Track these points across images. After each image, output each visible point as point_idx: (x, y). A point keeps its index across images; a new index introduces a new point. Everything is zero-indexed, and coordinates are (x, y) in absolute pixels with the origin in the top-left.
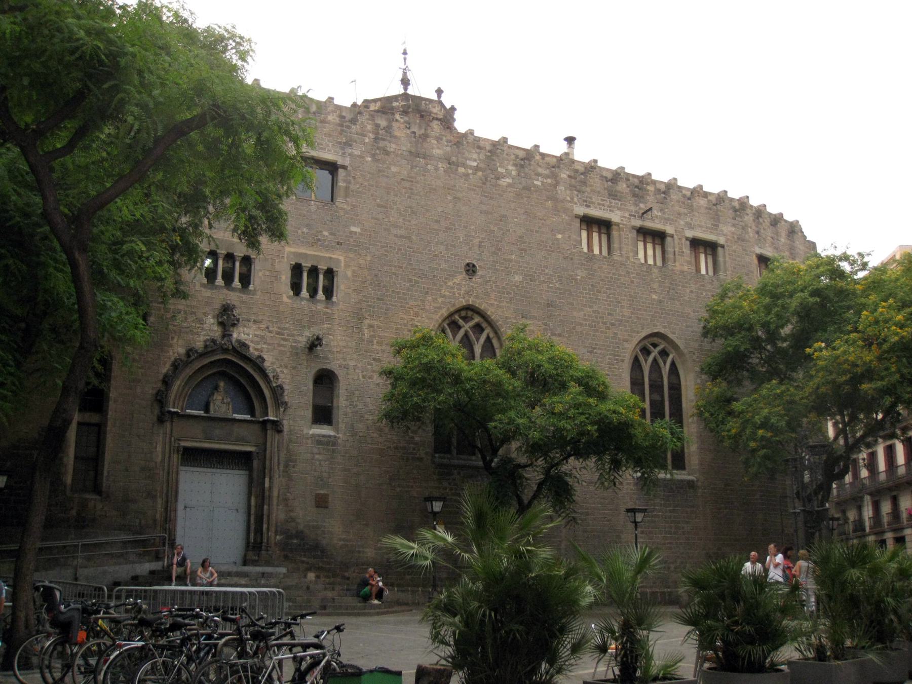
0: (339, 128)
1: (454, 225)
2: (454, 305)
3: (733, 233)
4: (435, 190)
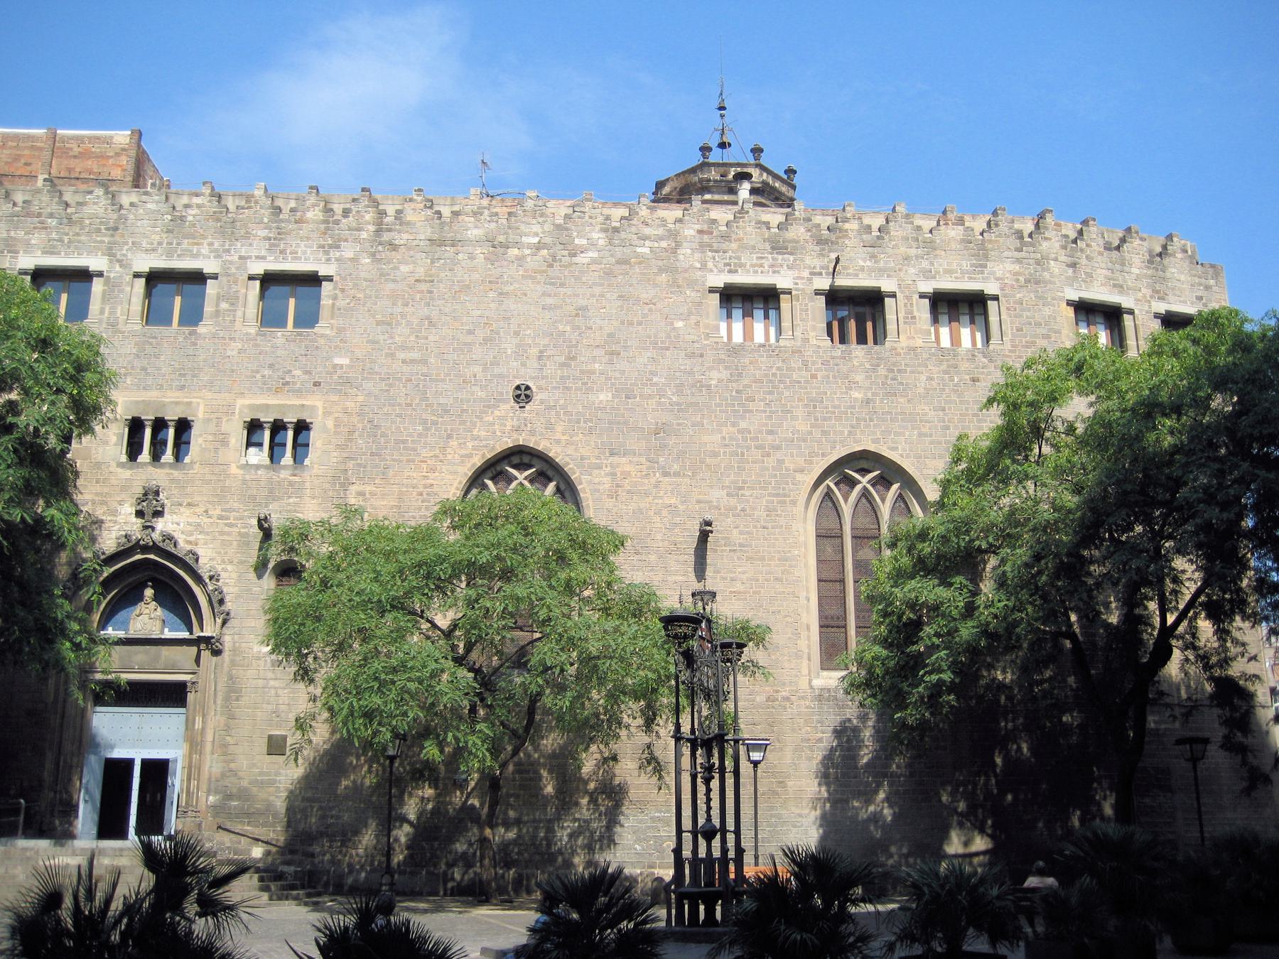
0: (323, 226)
1: (498, 333)
2: (493, 448)
3: (1016, 274)
4: (468, 287)
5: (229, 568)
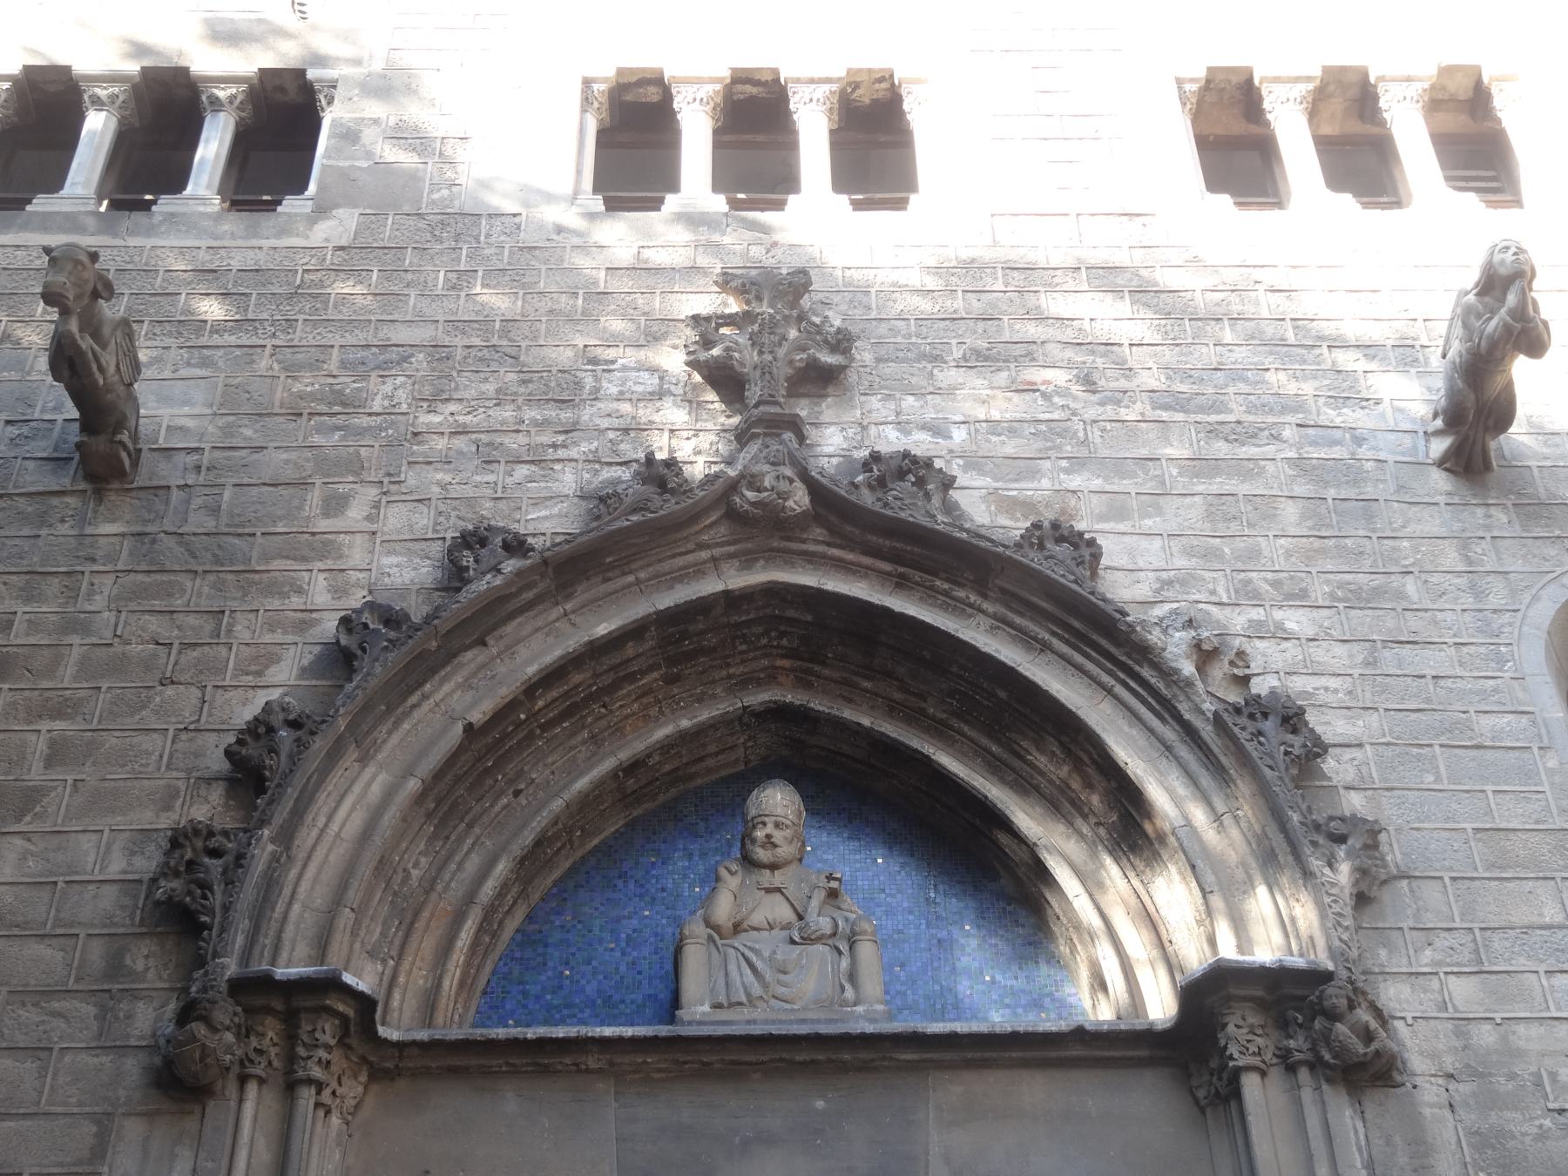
5: (1295, 620)
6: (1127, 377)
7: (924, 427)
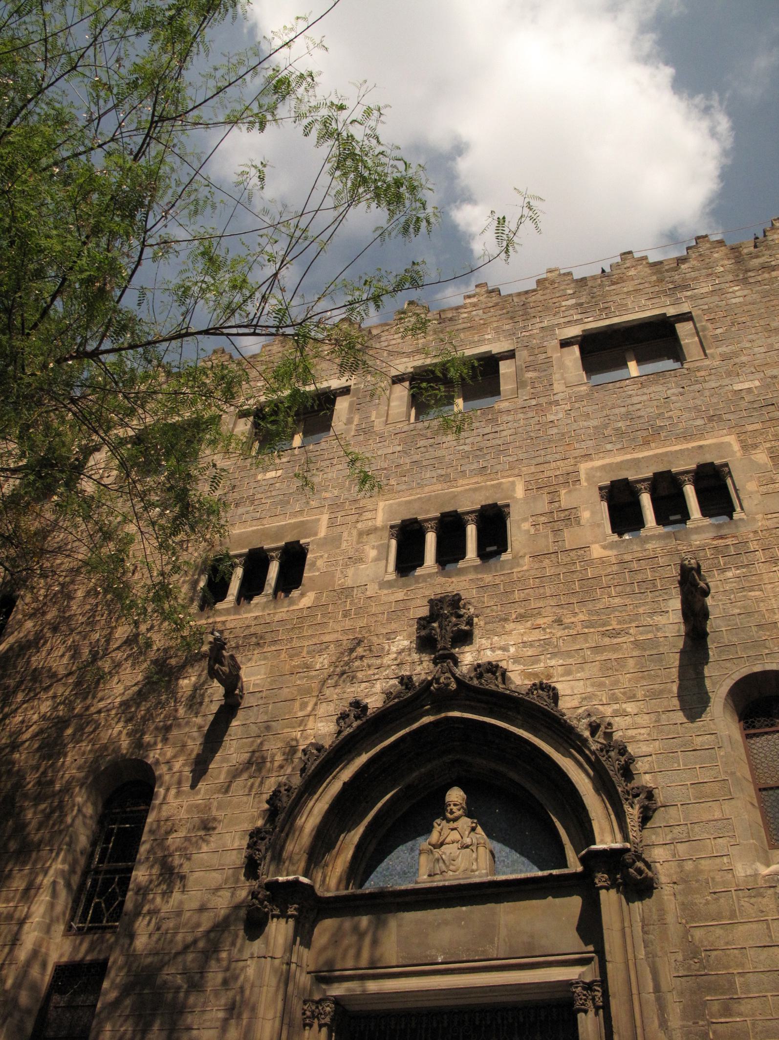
5: (630, 708)
6: (574, 617)
7: (500, 648)
